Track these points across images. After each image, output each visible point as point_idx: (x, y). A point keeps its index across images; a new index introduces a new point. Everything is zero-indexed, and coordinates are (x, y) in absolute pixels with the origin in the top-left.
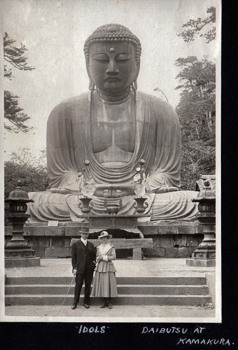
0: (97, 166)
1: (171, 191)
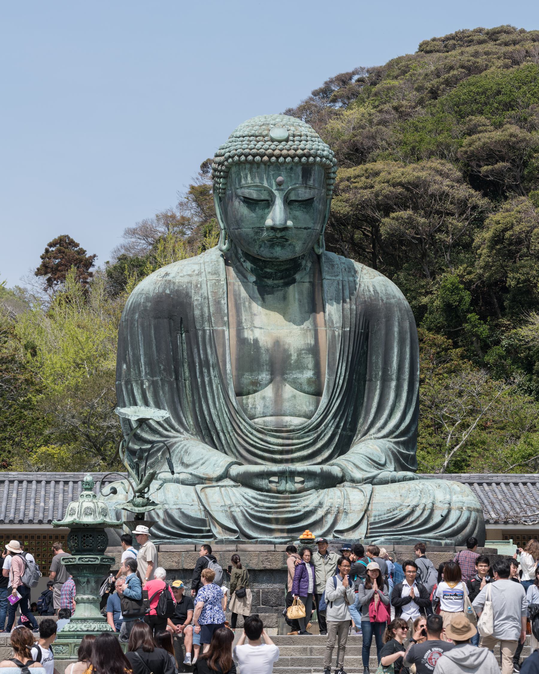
0: (246, 425)
1: (404, 479)
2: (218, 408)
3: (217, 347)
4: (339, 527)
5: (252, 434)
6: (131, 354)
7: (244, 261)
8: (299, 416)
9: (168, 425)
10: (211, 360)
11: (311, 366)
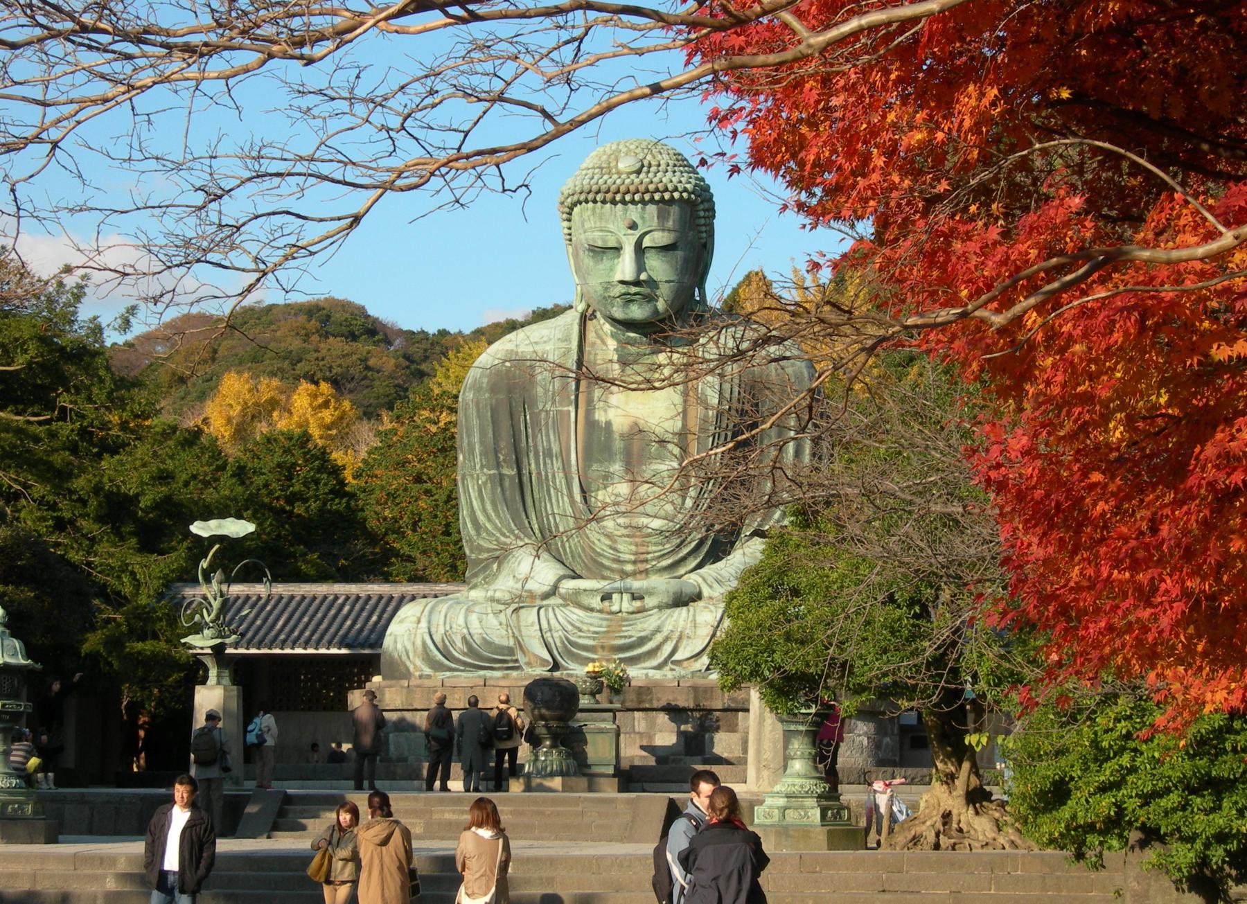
4: (677, 657)
10: (555, 449)
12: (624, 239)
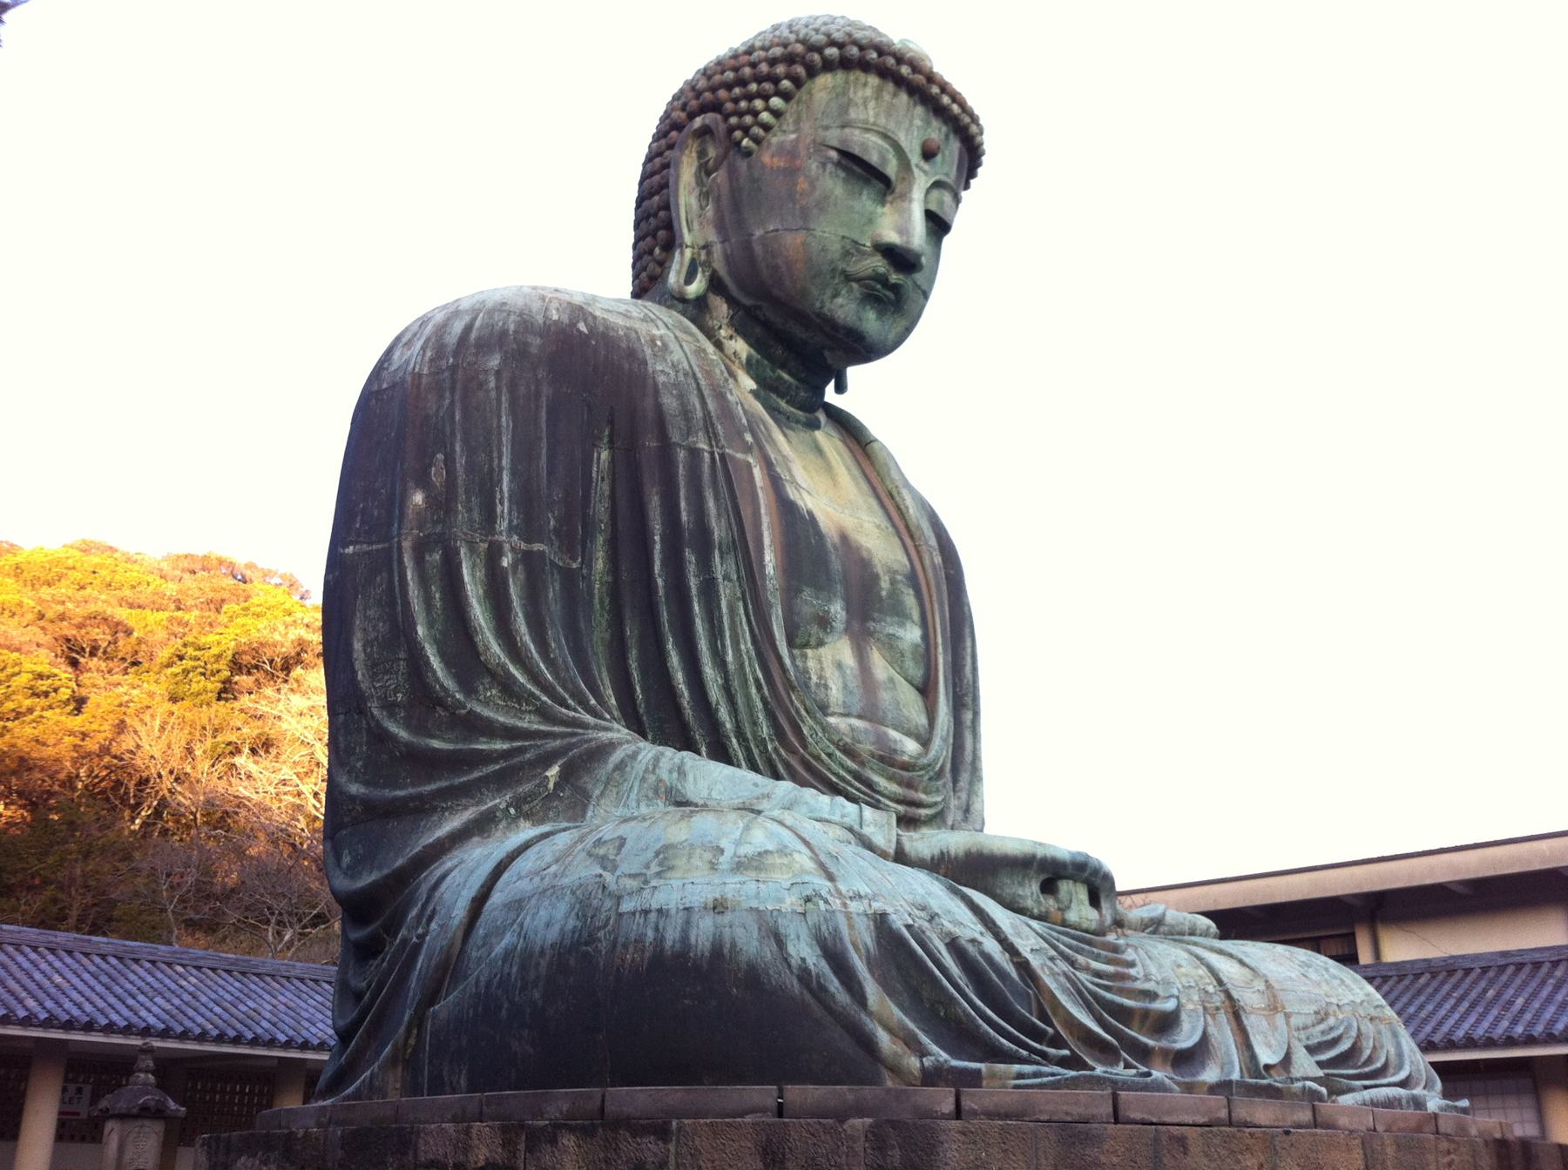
2: (732, 667)
3: (740, 502)
5: (830, 755)
6: (460, 461)
7: (731, 338)
8: (908, 734)
9: (564, 688)
10: (719, 530)
11: (916, 615)
12: (916, 170)
